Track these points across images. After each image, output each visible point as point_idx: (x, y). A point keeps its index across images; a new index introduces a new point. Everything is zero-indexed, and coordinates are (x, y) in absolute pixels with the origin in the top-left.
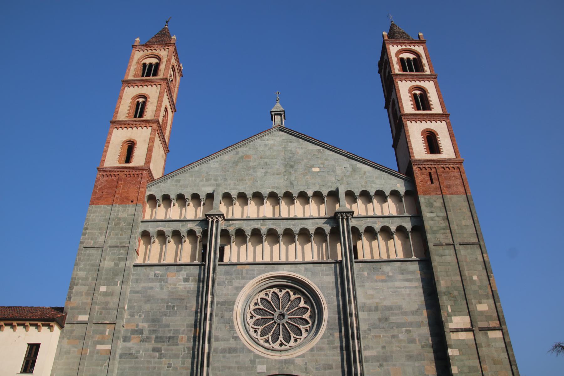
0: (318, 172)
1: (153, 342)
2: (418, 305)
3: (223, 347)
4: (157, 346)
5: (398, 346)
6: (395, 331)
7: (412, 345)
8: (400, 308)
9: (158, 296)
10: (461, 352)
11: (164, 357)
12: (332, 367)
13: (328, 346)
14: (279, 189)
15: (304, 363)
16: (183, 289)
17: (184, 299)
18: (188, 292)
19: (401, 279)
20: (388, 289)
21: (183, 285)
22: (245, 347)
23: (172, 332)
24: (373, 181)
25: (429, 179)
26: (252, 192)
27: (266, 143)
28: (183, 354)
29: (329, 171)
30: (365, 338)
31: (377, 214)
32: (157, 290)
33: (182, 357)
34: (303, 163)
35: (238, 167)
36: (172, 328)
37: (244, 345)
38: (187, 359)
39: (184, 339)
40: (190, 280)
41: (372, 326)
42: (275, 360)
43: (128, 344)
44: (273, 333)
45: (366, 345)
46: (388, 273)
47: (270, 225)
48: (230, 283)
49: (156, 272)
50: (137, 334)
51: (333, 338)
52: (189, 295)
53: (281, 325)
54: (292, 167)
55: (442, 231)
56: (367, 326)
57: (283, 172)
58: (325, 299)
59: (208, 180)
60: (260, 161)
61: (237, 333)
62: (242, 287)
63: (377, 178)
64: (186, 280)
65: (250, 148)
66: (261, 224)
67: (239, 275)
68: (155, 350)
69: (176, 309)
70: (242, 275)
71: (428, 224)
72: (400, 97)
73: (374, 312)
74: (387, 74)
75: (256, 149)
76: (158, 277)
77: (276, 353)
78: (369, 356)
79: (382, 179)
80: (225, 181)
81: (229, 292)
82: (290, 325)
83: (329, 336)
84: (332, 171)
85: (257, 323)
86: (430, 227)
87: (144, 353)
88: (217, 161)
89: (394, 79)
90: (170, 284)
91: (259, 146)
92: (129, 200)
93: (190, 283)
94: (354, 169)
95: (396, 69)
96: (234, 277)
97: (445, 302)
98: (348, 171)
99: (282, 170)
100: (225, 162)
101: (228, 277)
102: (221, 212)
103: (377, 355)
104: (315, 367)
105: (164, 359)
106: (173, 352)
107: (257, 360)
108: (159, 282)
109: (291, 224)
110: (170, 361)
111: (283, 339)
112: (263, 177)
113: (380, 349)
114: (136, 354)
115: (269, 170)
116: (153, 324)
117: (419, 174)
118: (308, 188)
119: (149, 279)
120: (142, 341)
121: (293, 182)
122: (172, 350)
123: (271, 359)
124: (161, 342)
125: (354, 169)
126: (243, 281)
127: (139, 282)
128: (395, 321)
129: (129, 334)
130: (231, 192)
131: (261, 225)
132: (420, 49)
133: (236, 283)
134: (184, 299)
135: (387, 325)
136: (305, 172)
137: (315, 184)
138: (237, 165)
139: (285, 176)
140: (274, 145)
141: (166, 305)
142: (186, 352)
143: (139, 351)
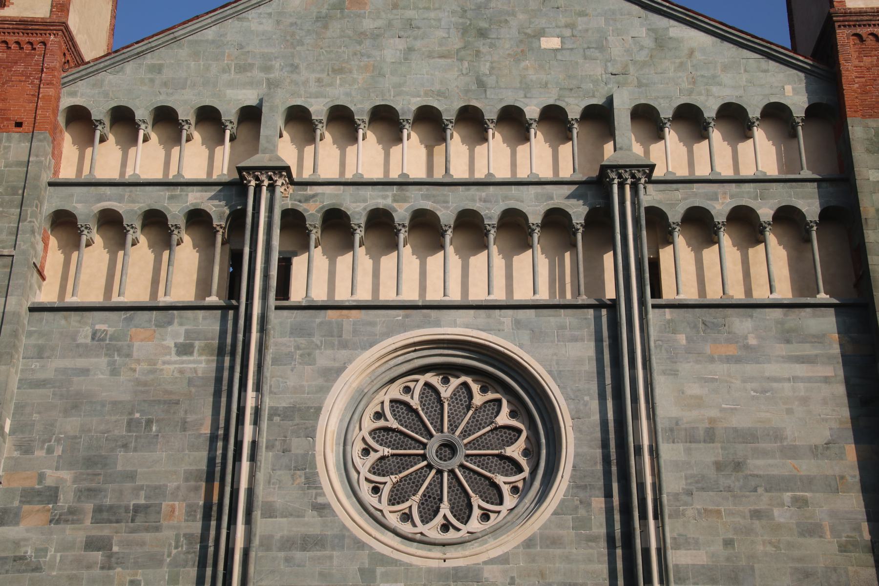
0: (557, 50)
1: (88, 522)
2: (831, 429)
3: (286, 533)
5: (770, 543)
6: (763, 501)
7: (813, 541)
8: (777, 435)
9: (104, 394)
11: (121, 563)
13: (573, 532)
14: (446, 98)
15: (508, 580)
16: (176, 375)
17: (177, 403)
19: (783, 357)
20: (744, 381)
21: (175, 362)
22: (347, 534)
23: (142, 493)
24: (714, 77)
26: (368, 106)
28: (172, 555)
29: (589, 48)
30: (676, 514)
31: (720, 174)
32: (102, 376)
33: (170, 564)
34: (514, 23)
35: (329, 34)
37: (344, 527)
38: (184, 567)
39: (177, 513)
40: (196, 348)
41: (697, 482)
42: (429, 570)
44: (424, 495)
45: (680, 535)
46: (746, 338)
47: (419, 200)
48: (308, 357)
49: (97, 327)
50: (40, 502)
51: (588, 512)
52: (193, 390)
53: (446, 475)
54: (482, 34)
56: (684, 482)
57: (458, 51)
58: (568, 405)
59: (243, 68)
61: (325, 495)
62: (340, 371)
63: (725, 68)
64: (184, 349)
66: (394, 196)
67: (332, 336)
68: (91, 544)
69: (154, 428)
70: (341, 336)
73: (702, 445)
76: (103, 340)
77: (430, 550)
78: (688, 565)
81: (305, 383)
82: (469, 474)
83: (577, 507)
84: (596, 48)
85: (381, 467)
87: (59, 555)
88: (270, 14)
90: (138, 361)
92: (8, 119)
93: (195, 356)
94: (661, 42)
96: (319, 343)
98: (642, 48)
99: (456, 42)
100: (291, 16)
101: (302, 341)
102: (283, 161)
103: (710, 563)
105: (119, 570)
107: (380, 570)
108: (106, 355)
109: (477, 198)
110: (136, 574)
111: (452, 512)
112: (400, 63)
113: (718, 547)
114: (35, 558)
115: (418, 44)
116: (89, 471)
118: (526, 97)
119: (78, 346)
120: (56, 520)
121: (485, 79)
122: (143, 544)
123: (417, 566)
124: (111, 522)
125: (661, 42)
126: (344, 353)
127: (46, 355)
128: (761, 473)
129: (16, 503)
130: (312, 105)
131: (395, 201)
133: (324, 358)
134: (177, 403)
135: (739, 481)
136: (519, 50)
138: (326, 27)
139: (461, 60)
141: (125, 418)
142: (182, 546)
143: (46, 550)
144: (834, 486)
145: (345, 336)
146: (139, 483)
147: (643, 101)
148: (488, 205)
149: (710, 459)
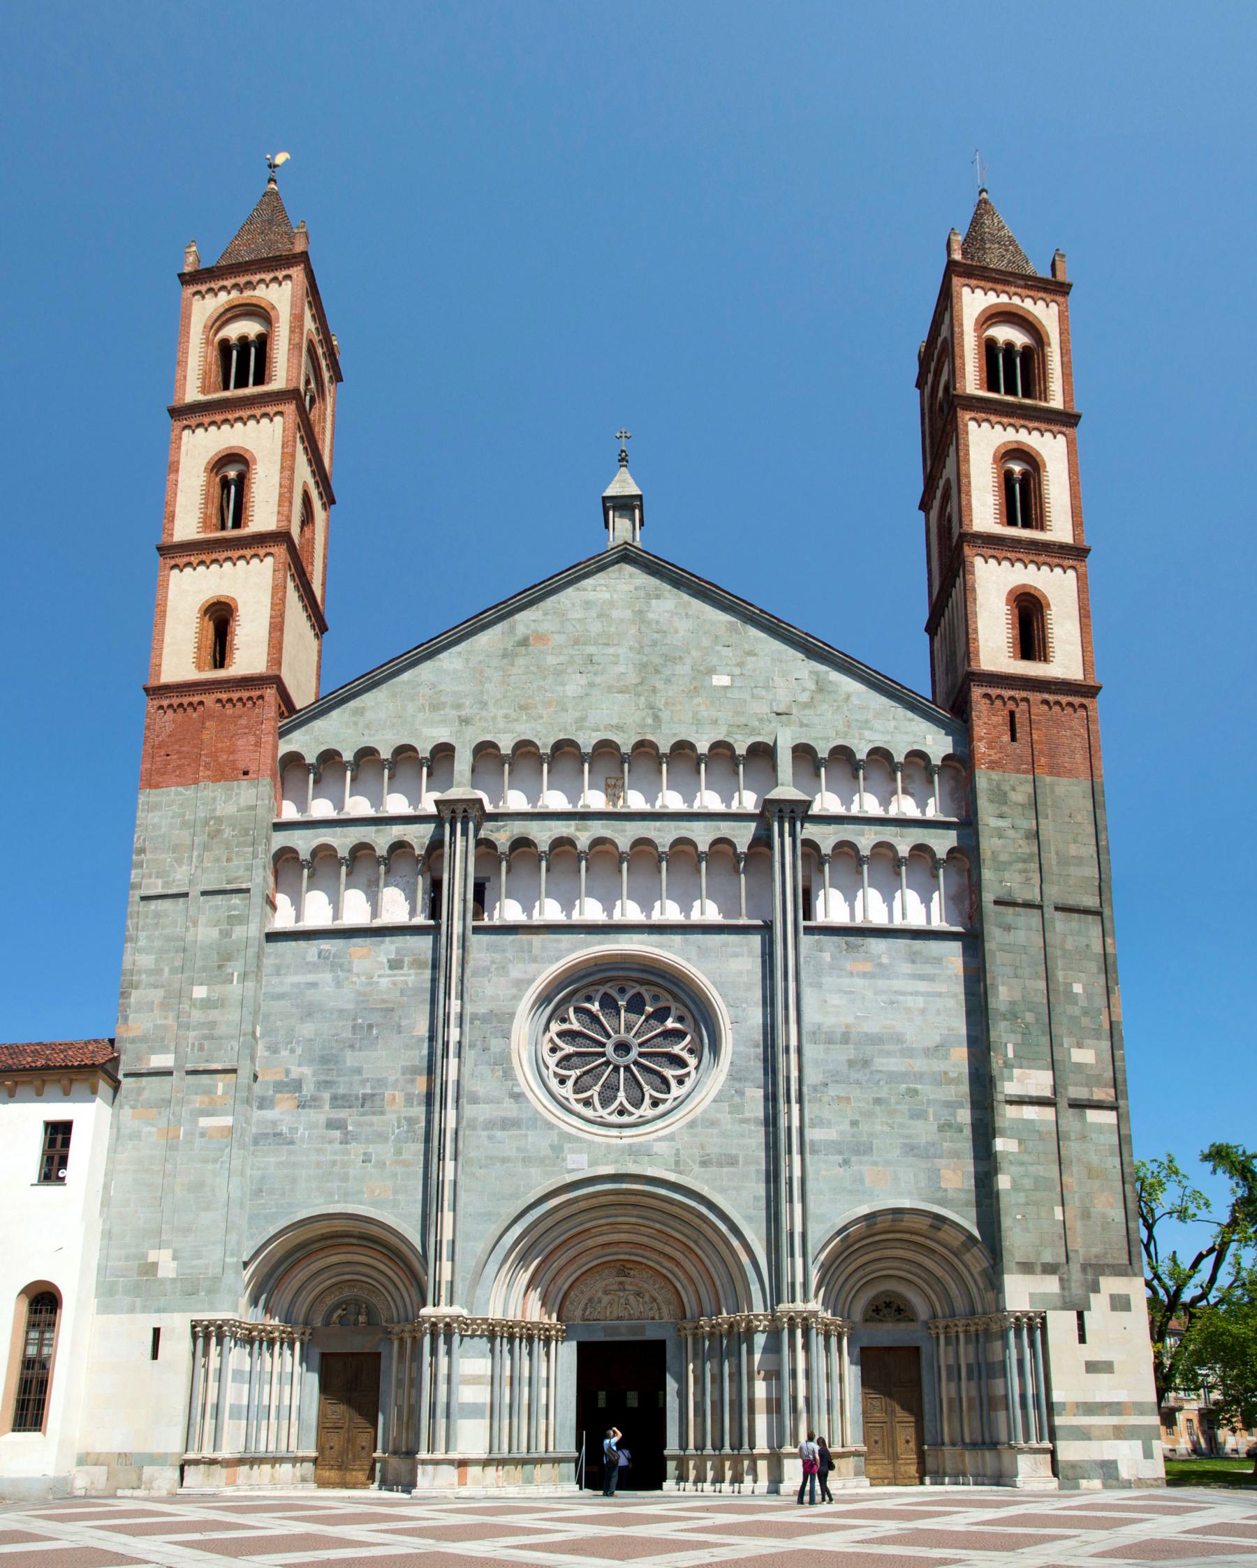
0: (726, 687)
4: (336, 1116)
5: (887, 1124)
7: (919, 1123)
8: (899, 1039)
10: (1022, 1146)
12: (737, 1162)
14: (623, 732)
18: (402, 993)
19: (909, 974)
20: (876, 994)
24: (867, 721)
25: (1007, 728)
27: (591, 597)
34: (688, 661)
36: (368, 1076)
43: (269, 1114)
45: (817, 1117)
46: (880, 957)
47: (600, 829)
48: (503, 970)
52: (405, 999)
55: (1020, 866)
57: (637, 685)
60: (574, 652)
65: (545, 614)
66: (577, 825)
71: (988, 845)
72: (968, 476)
73: (838, 1046)
74: (940, 394)
75: (563, 615)
79: (891, 718)
80: (482, 709)
81: (500, 992)
83: (732, 1096)
84: (763, 688)
86: (993, 853)
89: (960, 413)
91: (569, 605)
94: (821, 687)
95: (971, 381)
97: (1003, 1034)
99: (633, 678)
101: (497, 956)
104: (698, 1160)
106: (375, 1128)
113: (846, 1127)
115: (598, 680)
117: (986, 713)
120: (302, 1105)
126: (532, 967)
128: (884, 1069)
129: (271, 1092)
131: (577, 830)
132: (1045, 313)
133: (516, 971)
134: (392, 1010)
136: (692, 687)
137: (715, 722)
140: (611, 603)
144: (942, 1079)
145: (534, 951)
146: (365, 1076)
147: (804, 741)
148: (662, 834)
149: (844, 1057)
